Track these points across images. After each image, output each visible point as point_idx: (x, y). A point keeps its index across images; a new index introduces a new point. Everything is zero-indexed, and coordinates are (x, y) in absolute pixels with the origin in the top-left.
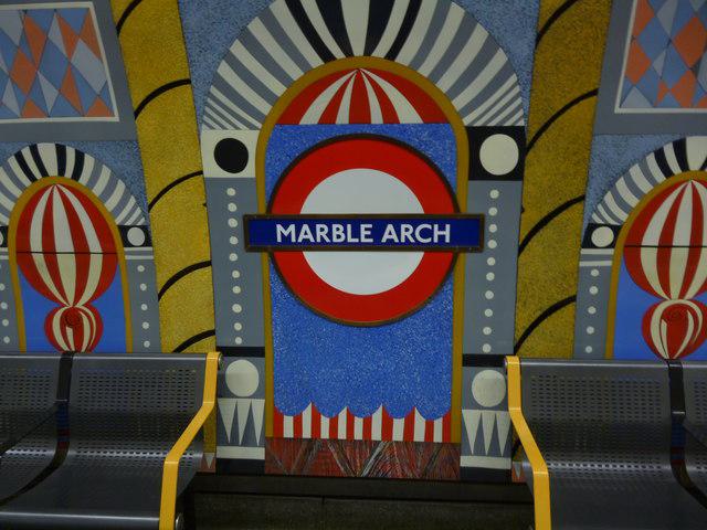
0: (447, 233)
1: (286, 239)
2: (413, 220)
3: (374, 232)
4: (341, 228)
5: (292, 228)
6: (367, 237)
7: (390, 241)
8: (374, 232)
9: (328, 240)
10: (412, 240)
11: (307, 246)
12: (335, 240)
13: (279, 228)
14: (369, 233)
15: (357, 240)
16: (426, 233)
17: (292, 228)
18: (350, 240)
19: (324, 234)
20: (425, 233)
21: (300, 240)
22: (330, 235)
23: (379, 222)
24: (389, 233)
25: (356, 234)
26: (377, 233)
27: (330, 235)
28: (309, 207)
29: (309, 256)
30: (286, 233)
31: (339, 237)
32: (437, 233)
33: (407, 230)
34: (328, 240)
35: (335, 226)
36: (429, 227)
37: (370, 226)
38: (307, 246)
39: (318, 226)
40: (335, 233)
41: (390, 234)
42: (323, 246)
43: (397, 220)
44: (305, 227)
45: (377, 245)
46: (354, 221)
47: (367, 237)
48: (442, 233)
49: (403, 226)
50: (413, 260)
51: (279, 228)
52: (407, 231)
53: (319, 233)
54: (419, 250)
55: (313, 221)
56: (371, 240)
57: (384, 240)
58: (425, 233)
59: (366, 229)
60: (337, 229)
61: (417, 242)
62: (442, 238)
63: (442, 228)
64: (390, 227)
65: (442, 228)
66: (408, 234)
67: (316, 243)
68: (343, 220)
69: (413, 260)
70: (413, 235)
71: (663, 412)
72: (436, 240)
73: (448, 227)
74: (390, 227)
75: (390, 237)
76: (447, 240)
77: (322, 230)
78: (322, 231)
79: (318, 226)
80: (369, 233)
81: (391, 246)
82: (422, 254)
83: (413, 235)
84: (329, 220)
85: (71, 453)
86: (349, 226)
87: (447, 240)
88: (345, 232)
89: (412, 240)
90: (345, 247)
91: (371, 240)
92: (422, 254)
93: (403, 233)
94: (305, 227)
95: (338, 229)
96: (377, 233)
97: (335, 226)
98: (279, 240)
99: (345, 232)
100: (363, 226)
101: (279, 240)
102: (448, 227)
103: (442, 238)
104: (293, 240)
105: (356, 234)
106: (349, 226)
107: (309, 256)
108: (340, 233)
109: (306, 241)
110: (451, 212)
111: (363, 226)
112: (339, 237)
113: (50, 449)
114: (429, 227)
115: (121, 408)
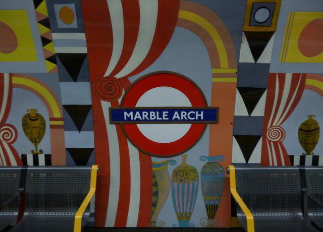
0: (202, 115)
1: (129, 118)
2: (187, 110)
3: (169, 115)
4: (154, 113)
5: (131, 113)
6: (166, 117)
7: (176, 119)
8: (169, 115)
9: (148, 119)
10: (186, 119)
11: (138, 121)
12: (151, 118)
13: (126, 113)
14: (167, 115)
15: (161, 119)
17: (131, 113)
18: (158, 118)
19: (146, 116)
20: (192, 115)
21: (135, 119)
22: (149, 116)
23: (171, 111)
24: (176, 115)
25: (161, 116)
27: (149, 116)
29: (138, 125)
30: (129, 116)
31: (153, 117)
32: (197, 115)
33: (184, 114)
34: (148, 119)
35: (151, 113)
36: (194, 112)
37: (167, 112)
38: (138, 121)
39: (144, 113)
40: (151, 116)
41: (176, 116)
42: (146, 121)
43: (180, 110)
44: (138, 113)
45: (170, 121)
46: (160, 110)
47: (166, 117)
48: (199, 115)
49: (182, 112)
50: (186, 128)
51: (126, 113)
52: (184, 115)
53: (144, 116)
54: (188, 123)
55: (141, 110)
56: (167, 119)
57: (173, 119)
58: (192, 115)
59: (165, 114)
60: (152, 114)
61: (189, 119)
62: (199, 117)
63: (200, 113)
64: (176, 113)
65: (200, 113)
66: (185, 116)
67: (142, 120)
68: (155, 109)
69: (186, 128)
70: (187, 116)
72: (197, 118)
73: (202, 112)
74: (176, 113)
75: (176, 117)
76: (202, 118)
77: (145, 114)
78: (145, 115)
79: (144, 113)
80: (167, 115)
81: (177, 121)
83: (187, 116)
84: (149, 110)
85: (26, 214)
86: (158, 113)
87: (202, 118)
88: (156, 115)
89: (186, 119)
90: (156, 122)
91: (167, 119)
93: (182, 115)
94: (138, 113)
95: (152, 114)
97: (151, 113)
98: (125, 119)
99: (156, 115)
100: (164, 113)
101: (125, 119)
102: (202, 112)
103: (199, 117)
104: (132, 119)
105: (161, 116)
106: (158, 113)
107: (138, 125)
108: (154, 115)
109: (138, 119)
110: (203, 107)
111: (164, 113)
112: (153, 117)
113: (15, 212)
114: (194, 112)
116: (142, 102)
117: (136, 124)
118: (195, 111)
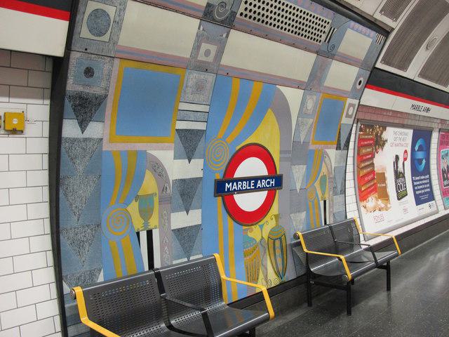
0: (273, 182)
1: (229, 189)
3: (253, 183)
16: (269, 183)
18: (248, 188)
22: (242, 186)
23: (256, 179)
25: (250, 186)
26: (256, 184)
27: (242, 186)
28: (238, 174)
29: (237, 197)
32: (271, 183)
42: (240, 191)
45: (257, 189)
46: (248, 179)
50: (265, 193)
55: (237, 180)
69: (265, 193)
81: (260, 189)
82: (267, 192)
84: (242, 180)
90: (247, 191)
92: (267, 192)
93: (263, 184)
96: (256, 184)
105: (250, 186)
115: (151, 303)
116: (238, 174)
118: (269, 178)
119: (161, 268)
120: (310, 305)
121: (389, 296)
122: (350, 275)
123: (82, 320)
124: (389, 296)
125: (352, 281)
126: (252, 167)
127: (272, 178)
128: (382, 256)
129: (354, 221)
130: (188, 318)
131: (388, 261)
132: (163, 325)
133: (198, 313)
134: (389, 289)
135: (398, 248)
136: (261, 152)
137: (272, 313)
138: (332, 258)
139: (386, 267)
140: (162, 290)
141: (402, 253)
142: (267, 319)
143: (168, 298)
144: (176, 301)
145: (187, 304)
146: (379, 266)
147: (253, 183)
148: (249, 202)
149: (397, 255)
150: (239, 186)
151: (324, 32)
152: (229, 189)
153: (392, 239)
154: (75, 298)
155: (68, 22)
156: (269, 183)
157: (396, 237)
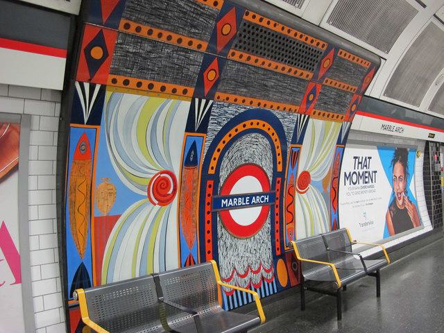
1: (225, 205)
2: (260, 194)
3: (248, 200)
16: (263, 199)
22: (237, 203)
23: (251, 196)
25: (245, 202)
27: (237, 203)
28: (234, 191)
29: (233, 213)
32: (265, 199)
42: (236, 207)
43: (256, 195)
44: (231, 200)
45: (251, 205)
46: (244, 196)
50: (259, 209)
71: (323, 250)
82: (260, 208)
84: (237, 196)
90: (242, 207)
92: (260, 208)
94: (231, 200)
105: (245, 202)
116: (234, 191)
117: (228, 210)
119: (160, 273)
120: (303, 309)
121: (379, 301)
122: (340, 282)
123: (83, 319)
124: (379, 301)
125: (344, 286)
126: (249, 184)
127: (266, 195)
128: (371, 265)
129: (346, 231)
130: (180, 320)
131: (378, 269)
132: (160, 326)
133: (191, 316)
134: (378, 295)
135: (388, 259)
136: (256, 171)
137: (263, 318)
138: (326, 265)
139: (376, 274)
140: (159, 293)
141: (391, 261)
142: (258, 323)
143: (166, 301)
144: (172, 304)
145: (182, 308)
146: (371, 274)
147: (248, 200)
148: (245, 216)
149: (386, 264)
150: (235, 202)
151: (317, 61)
152: (225, 205)
153: (382, 252)
154: (78, 299)
155: (65, 59)
156: (263, 199)
157: (386, 249)
